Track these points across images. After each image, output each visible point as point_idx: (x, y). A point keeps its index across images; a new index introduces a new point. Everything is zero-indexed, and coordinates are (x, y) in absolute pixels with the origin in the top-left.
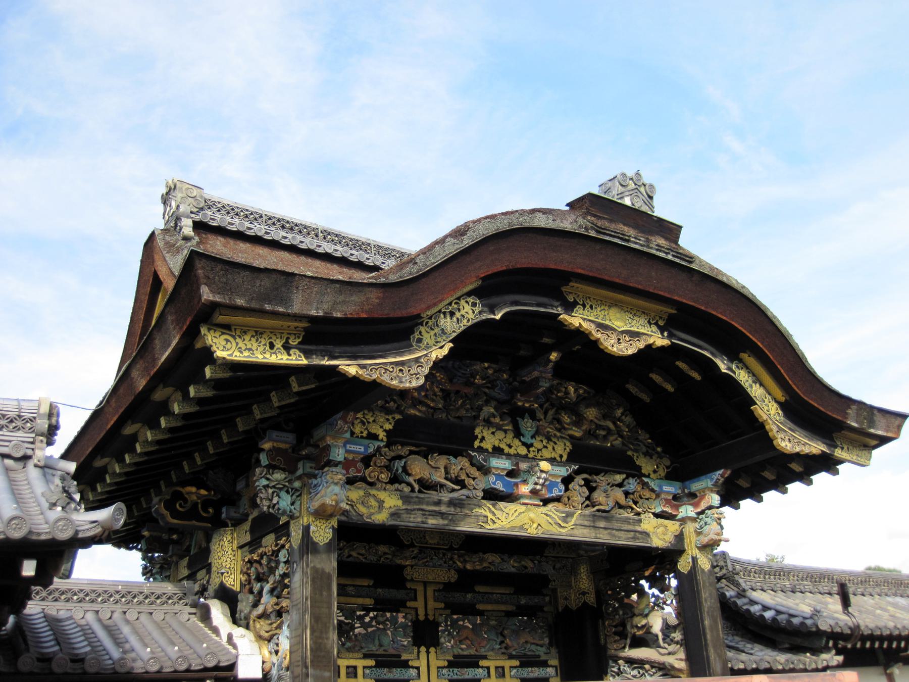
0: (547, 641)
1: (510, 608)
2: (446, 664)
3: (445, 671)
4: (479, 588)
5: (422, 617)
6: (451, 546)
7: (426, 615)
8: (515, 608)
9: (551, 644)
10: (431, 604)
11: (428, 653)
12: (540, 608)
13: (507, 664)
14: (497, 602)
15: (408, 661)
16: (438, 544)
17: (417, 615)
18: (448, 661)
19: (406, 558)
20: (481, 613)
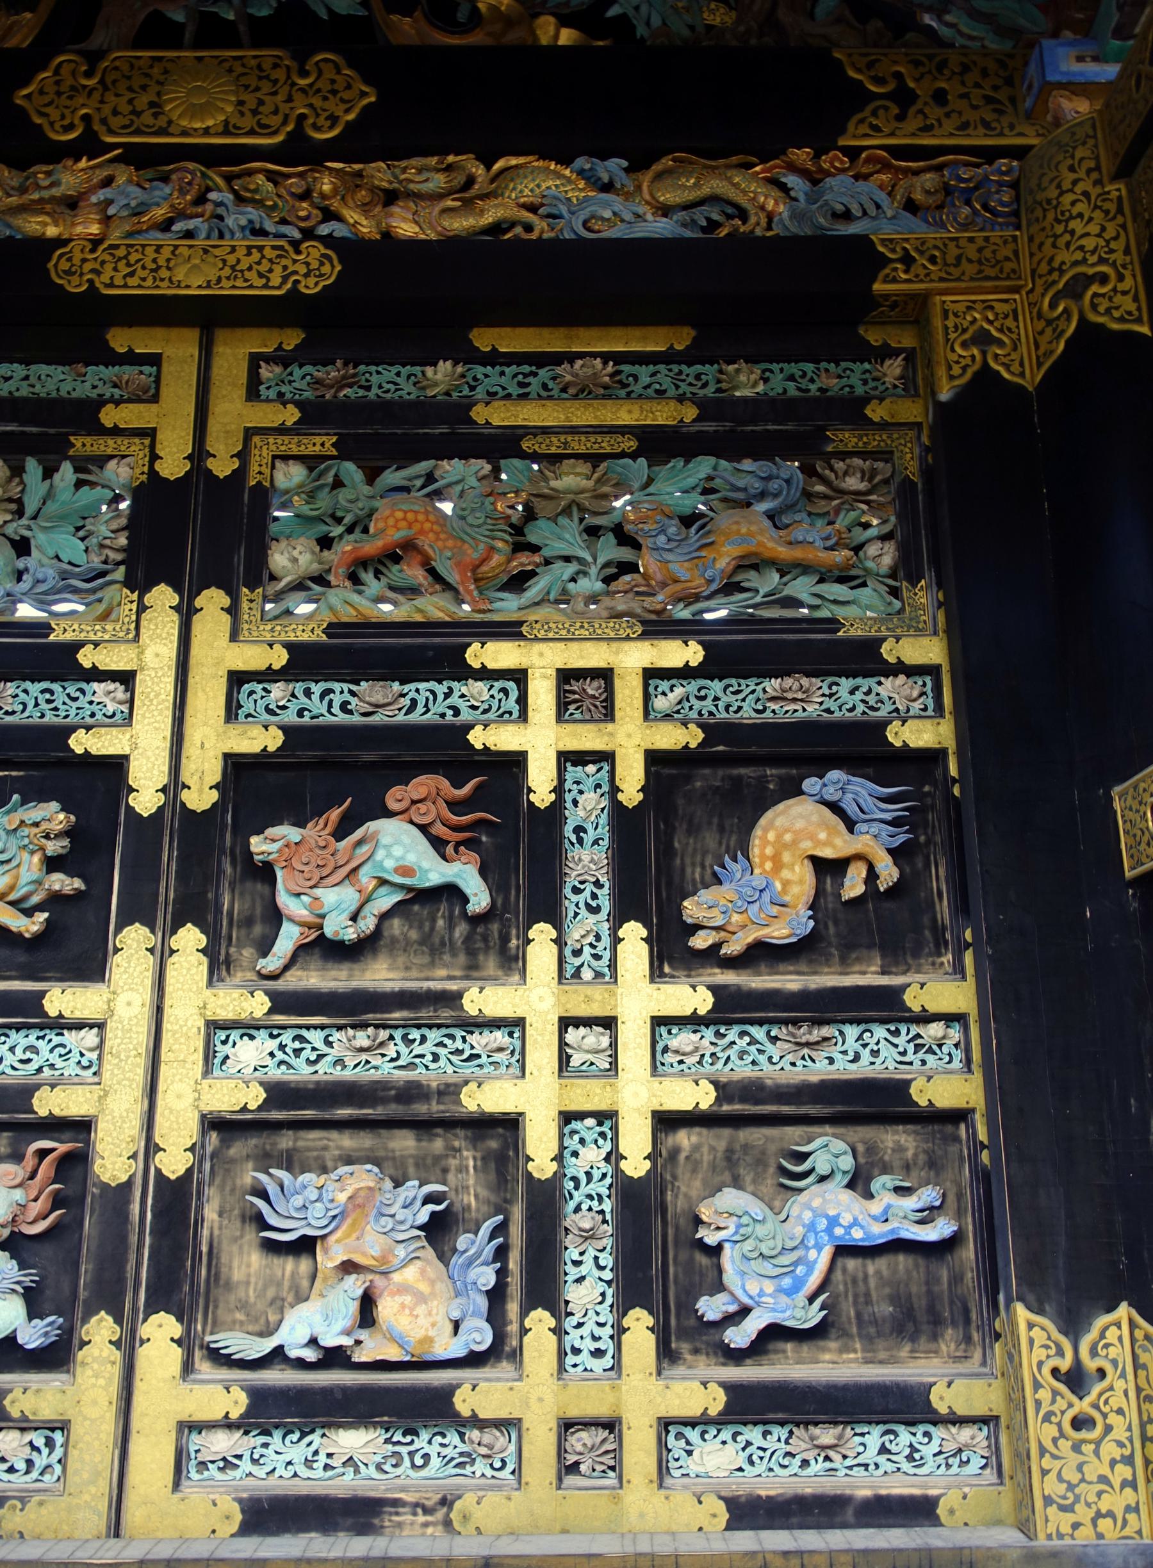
0: (882, 557)
1: (663, 415)
2: (279, 658)
3: (278, 691)
4: (483, 339)
5: (173, 466)
6: (298, 135)
7: (199, 454)
8: (690, 413)
9: (907, 569)
10: (232, 412)
11: (187, 613)
12: (851, 410)
13: (633, 658)
14: (584, 392)
15: (78, 645)
16: (226, 132)
17: (154, 457)
18: (289, 646)
19: (72, 204)
20: (502, 446)
